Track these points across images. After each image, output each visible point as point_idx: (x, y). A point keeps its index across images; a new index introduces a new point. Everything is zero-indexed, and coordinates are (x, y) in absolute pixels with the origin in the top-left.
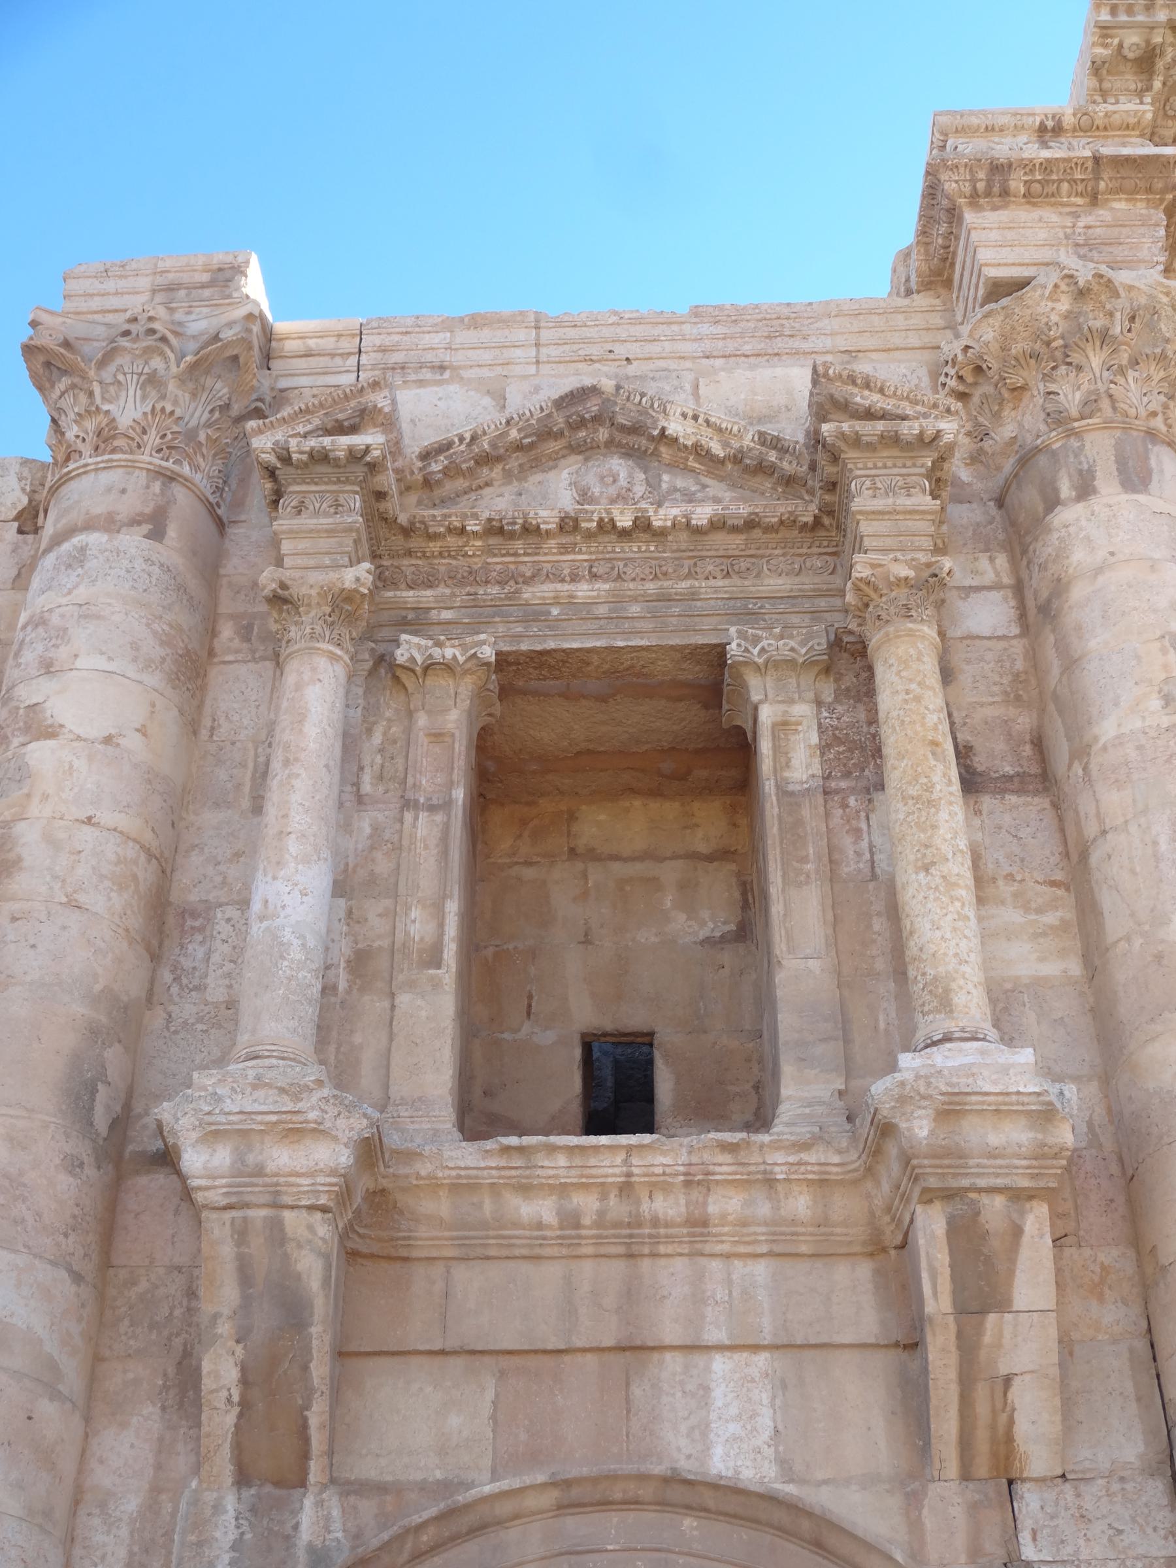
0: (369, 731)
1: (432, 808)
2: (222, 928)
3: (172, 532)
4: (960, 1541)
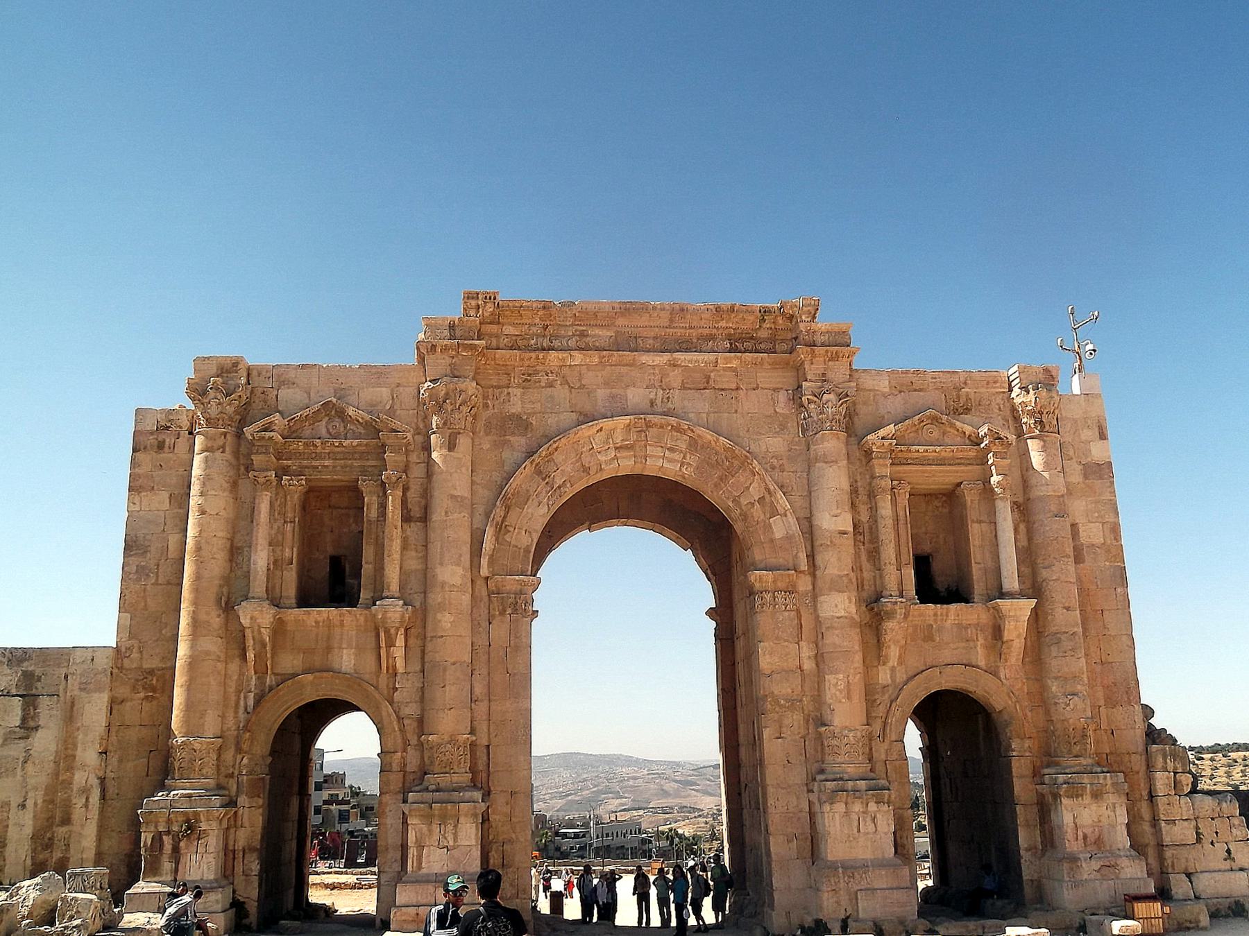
0: (277, 500)
1: (291, 522)
2: (246, 553)
3: (227, 449)
4: (385, 683)
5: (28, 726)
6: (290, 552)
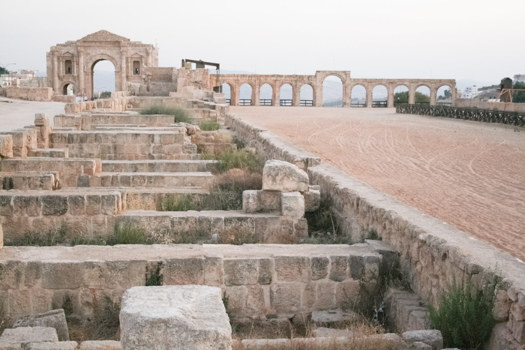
5: (39, 86)
6: (64, 68)
